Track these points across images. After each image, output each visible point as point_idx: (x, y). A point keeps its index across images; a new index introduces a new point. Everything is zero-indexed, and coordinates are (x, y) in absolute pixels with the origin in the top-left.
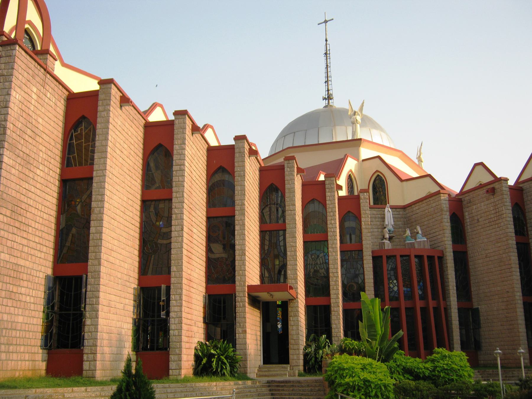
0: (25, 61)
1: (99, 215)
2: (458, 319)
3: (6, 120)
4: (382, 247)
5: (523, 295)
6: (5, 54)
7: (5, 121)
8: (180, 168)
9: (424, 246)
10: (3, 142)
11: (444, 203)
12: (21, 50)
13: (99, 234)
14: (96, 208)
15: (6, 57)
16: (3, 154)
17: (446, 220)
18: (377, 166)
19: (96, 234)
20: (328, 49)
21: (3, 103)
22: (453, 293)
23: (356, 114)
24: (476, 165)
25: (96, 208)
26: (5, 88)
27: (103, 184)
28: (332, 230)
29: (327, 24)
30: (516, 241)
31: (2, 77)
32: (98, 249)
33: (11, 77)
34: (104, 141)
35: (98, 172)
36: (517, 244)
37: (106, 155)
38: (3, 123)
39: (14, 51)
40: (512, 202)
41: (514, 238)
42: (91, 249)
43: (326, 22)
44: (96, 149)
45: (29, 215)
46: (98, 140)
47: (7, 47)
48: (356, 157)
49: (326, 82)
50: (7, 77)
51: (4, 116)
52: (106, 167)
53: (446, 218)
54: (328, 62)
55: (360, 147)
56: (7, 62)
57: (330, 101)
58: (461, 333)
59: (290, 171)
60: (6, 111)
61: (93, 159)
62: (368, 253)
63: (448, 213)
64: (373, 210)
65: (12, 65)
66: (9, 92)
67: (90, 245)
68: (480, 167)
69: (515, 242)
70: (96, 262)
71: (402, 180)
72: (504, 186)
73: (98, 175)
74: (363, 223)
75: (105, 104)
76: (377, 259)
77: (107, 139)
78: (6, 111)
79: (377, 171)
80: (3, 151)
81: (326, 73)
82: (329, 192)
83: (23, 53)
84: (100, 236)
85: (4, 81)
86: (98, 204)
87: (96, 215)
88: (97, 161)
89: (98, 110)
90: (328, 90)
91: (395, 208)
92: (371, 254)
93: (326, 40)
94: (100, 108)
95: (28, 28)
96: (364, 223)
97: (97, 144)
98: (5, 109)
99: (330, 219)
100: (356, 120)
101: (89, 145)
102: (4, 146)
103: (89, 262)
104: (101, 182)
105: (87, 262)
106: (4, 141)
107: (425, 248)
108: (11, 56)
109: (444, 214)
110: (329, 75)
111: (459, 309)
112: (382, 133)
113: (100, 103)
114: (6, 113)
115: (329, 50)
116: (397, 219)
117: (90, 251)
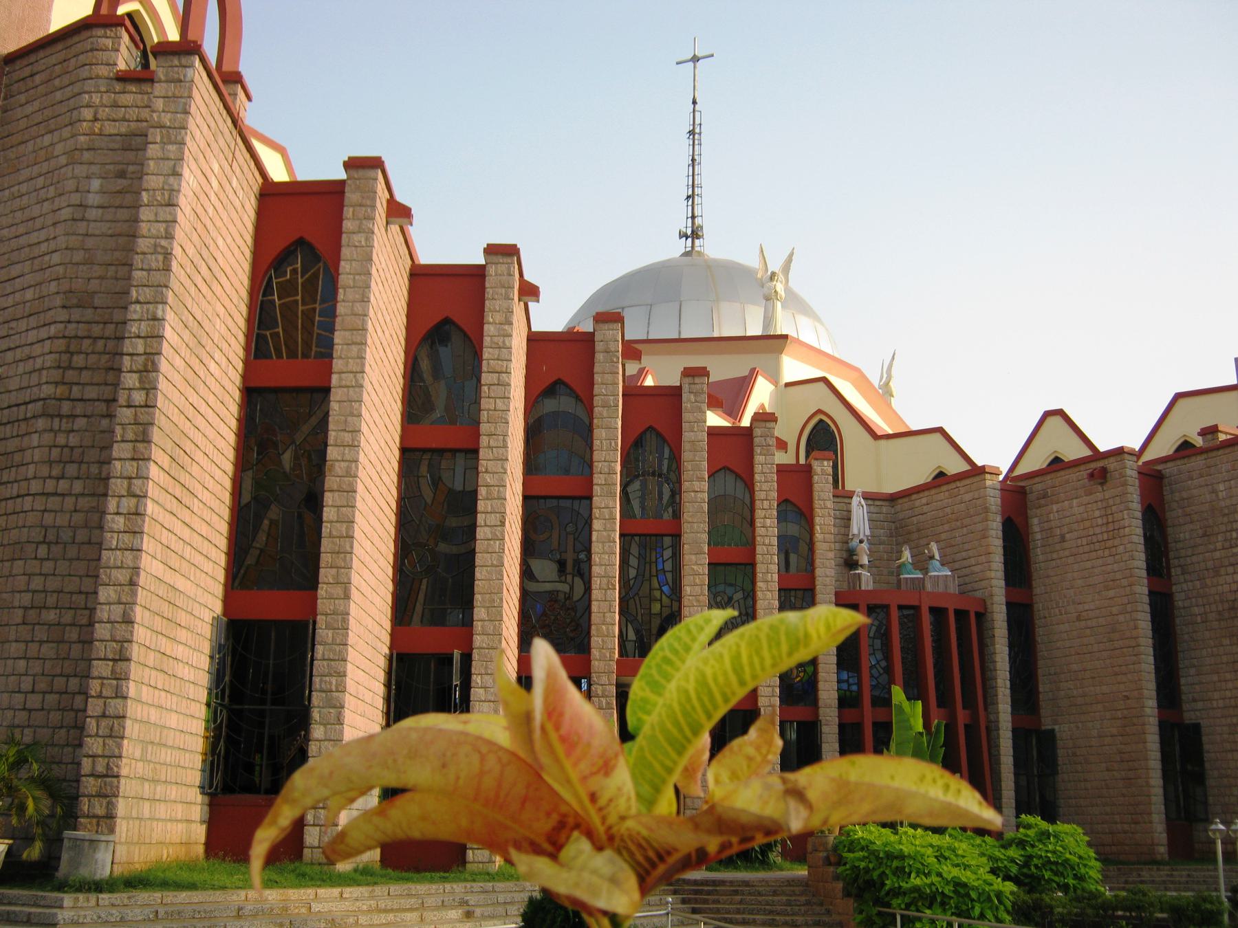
0: (206, 96)
1: (346, 479)
3: (169, 236)
4: (854, 585)
5: (1160, 706)
6: (166, 75)
7: (166, 238)
8: (499, 379)
10: (164, 289)
12: (201, 69)
13: (345, 525)
14: (338, 461)
15: (167, 81)
16: (164, 319)
18: (819, 399)
19: (338, 525)
20: (697, 122)
21: (163, 194)
24: (1047, 414)
25: (338, 461)
26: (168, 159)
27: (356, 405)
28: (767, 542)
29: (698, 64)
30: (1149, 586)
31: (158, 130)
32: (345, 560)
33: (183, 131)
34: (358, 304)
35: (343, 375)
36: (1151, 593)
37: (365, 336)
38: (163, 243)
39: (190, 72)
40: (1142, 502)
41: (1146, 581)
42: (325, 558)
43: (695, 59)
44: (338, 320)
45: (195, 469)
46: (343, 301)
47: (171, 57)
48: (774, 378)
49: (688, 197)
50: (171, 131)
51: (164, 225)
52: (363, 365)
54: (696, 153)
56: (170, 94)
57: (697, 242)
58: (1016, 783)
59: (696, 401)
60: (170, 213)
61: (330, 345)
63: (999, 518)
65: (185, 104)
66: (178, 169)
67: (322, 549)
68: (1055, 422)
69: (1145, 590)
70: (338, 591)
71: (875, 436)
73: (344, 383)
74: (818, 528)
75: (361, 216)
77: (365, 300)
78: (170, 213)
79: (819, 411)
80: (163, 311)
81: (691, 178)
82: (760, 454)
83: (204, 75)
84: (347, 528)
85: (165, 140)
86: (344, 454)
87: (338, 479)
88: (342, 349)
89: (344, 230)
90: (693, 217)
93: (694, 102)
94: (348, 225)
95: (138, 12)
97: (341, 309)
98: (168, 209)
99: (762, 516)
101: (314, 309)
102: (167, 298)
103: (319, 591)
104: (351, 401)
105: (316, 588)
106: (166, 286)
108: (181, 81)
111: (1014, 731)
112: (817, 324)
113: (348, 212)
114: (169, 218)
117: (322, 564)
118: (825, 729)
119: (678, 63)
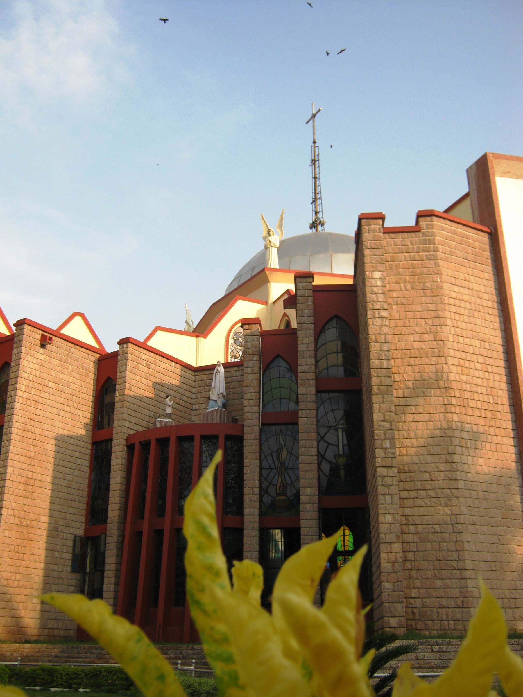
2: (257, 548)
9: (212, 420)
11: (249, 341)
17: (250, 370)
20: (317, 153)
22: (251, 501)
23: (271, 233)
43: (314, 116)
49: (314, 201)
53: (251, 365)
54: (317, 173)
55: (269, 282)
62: (119, 440)
64: (202, 373)
72: (301, 288)
76: (130, 448)
91: (236, 366)
92: (124, 442)
93: (314, 142)
96: (119, 393)
100: (270, 242)
107: (214, 422)
109: (247, 359)
110: (318, 192)
115: (318, 154)
116: (239, 383)
118: (109, 540)
119: (307, 123)
